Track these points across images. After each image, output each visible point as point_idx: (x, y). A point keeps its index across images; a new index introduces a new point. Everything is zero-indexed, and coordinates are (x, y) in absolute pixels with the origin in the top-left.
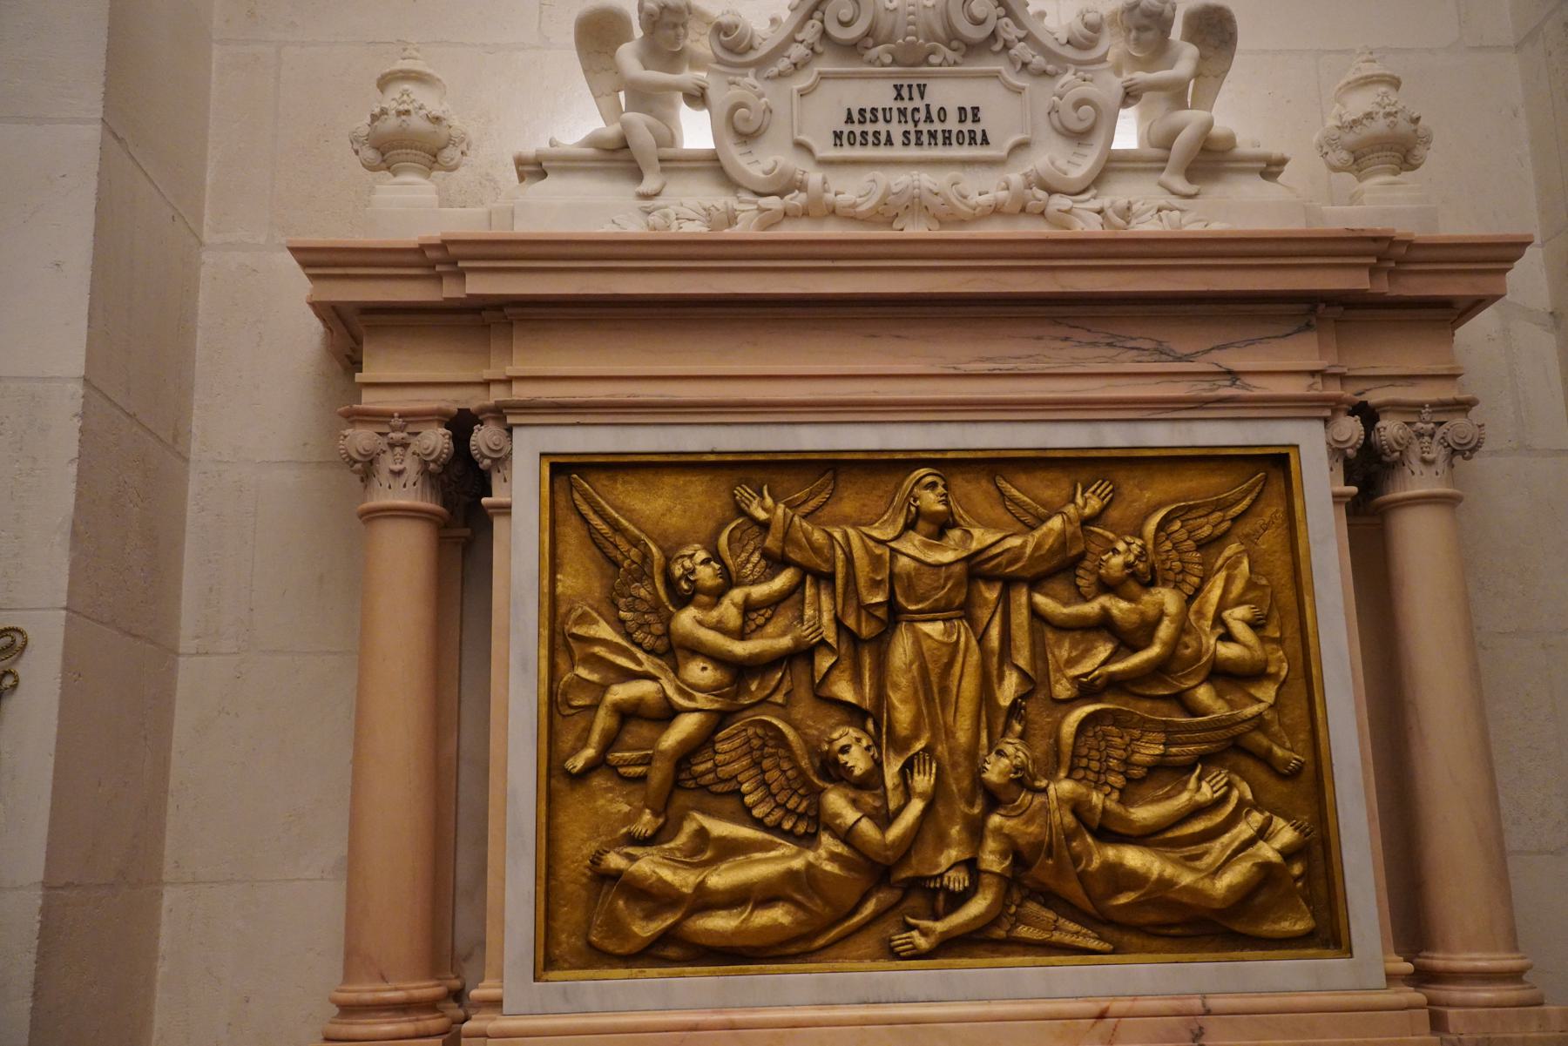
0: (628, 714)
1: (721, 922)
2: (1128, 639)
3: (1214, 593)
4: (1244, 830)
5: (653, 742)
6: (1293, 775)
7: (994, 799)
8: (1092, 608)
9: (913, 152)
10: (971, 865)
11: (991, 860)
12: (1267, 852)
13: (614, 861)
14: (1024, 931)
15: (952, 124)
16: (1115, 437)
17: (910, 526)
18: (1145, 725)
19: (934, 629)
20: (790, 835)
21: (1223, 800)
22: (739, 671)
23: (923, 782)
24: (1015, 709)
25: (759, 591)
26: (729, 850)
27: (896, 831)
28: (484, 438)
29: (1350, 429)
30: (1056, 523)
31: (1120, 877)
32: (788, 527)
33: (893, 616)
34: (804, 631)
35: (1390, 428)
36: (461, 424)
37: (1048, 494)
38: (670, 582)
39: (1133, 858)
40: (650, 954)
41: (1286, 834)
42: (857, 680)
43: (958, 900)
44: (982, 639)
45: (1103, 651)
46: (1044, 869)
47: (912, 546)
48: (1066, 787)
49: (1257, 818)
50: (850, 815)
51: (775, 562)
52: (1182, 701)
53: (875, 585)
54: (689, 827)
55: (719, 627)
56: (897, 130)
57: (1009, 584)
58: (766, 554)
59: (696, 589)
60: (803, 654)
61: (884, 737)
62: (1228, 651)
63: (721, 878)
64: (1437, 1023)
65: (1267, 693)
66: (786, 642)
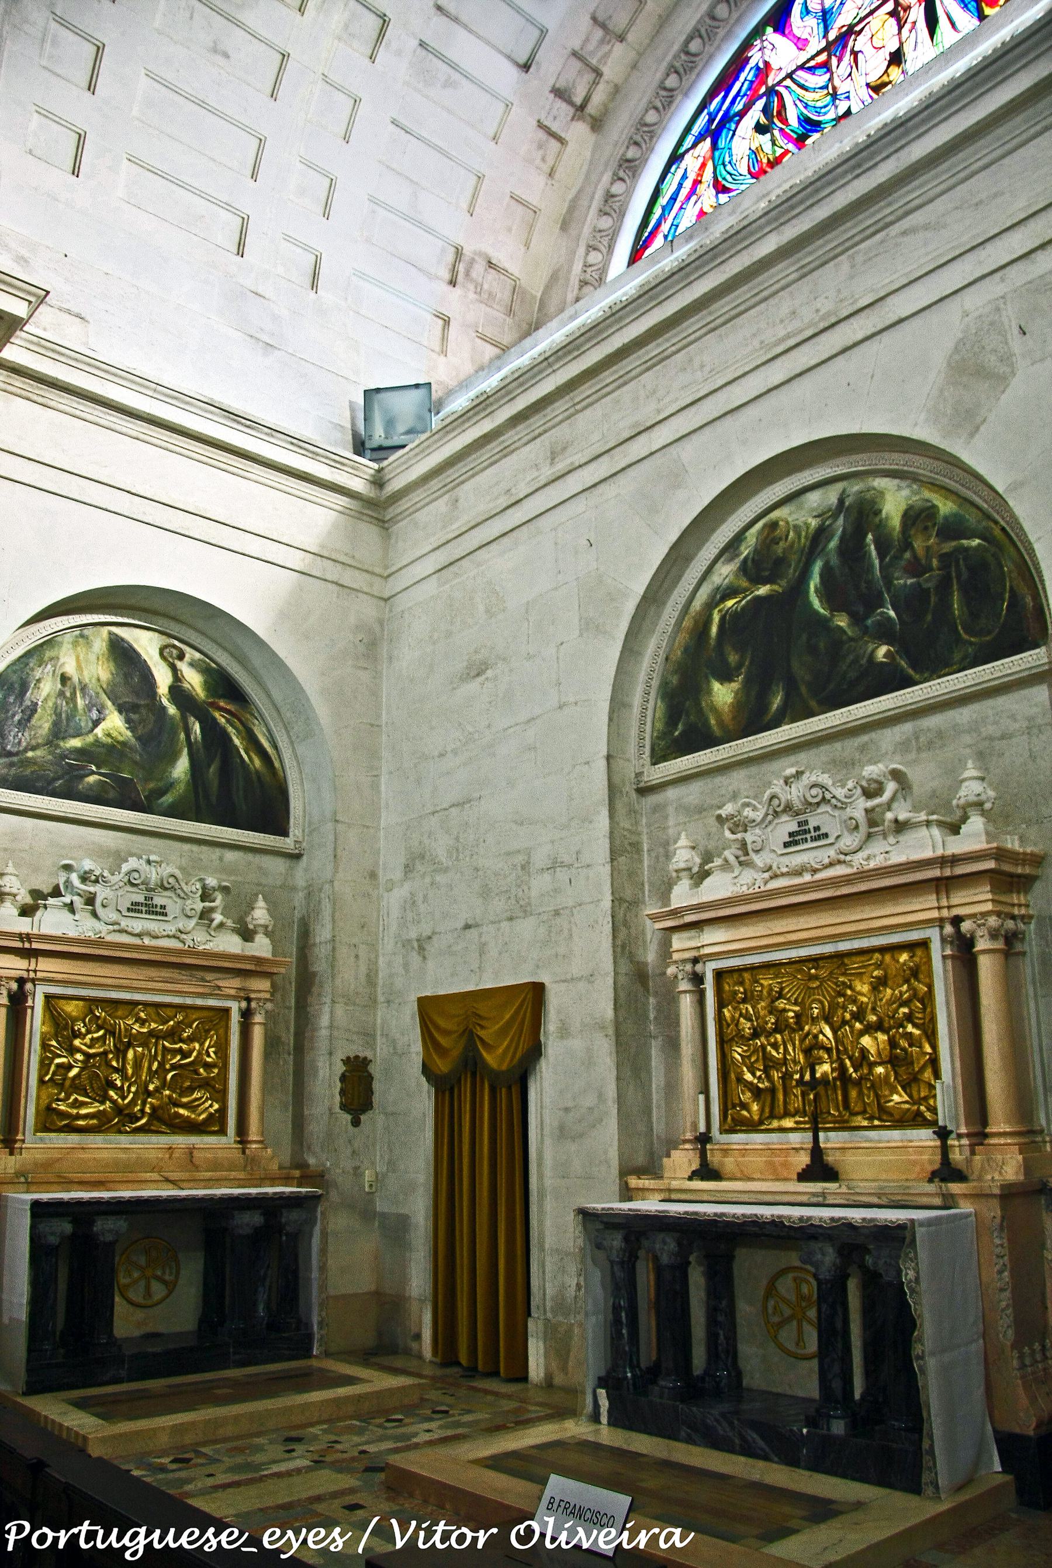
0: (59, 1066)
1: (81, 1123)
2: (185, 1055)
3: (207, 1044)
4: (207, 1104)
5: (66, 1075)
6: (218, 1092)
7: (149, 1094)
8: (177, 1046)
9: (147, 916)
10: (142, 1111)
11: (148, 1110)
12: (212, 1110)
13: (54, 1106)
14: (153, 1128)
15: (158, 910)
16: (189, 1001)
17: (136, 1021)
18: (187, 1078)
19: (140, 1049)
20: (98, 1101)
21: (201, 1098)
22: (88, 1056)
23: (133, 1089)
24: (156, 1071)
25: (95, 1035)
26: (83, 1104)
27: (126, 1101)
28: (29, 986)
29: (244, 1004)
30: (172, 1023)
31: (177, 1114)
32: (105, 1018)
33: (129, 1045)
34: (107, 1047)
35: (253, 1004)
36: (21, 981)
37: (170, 1014)
38: (73, 1030)
39: (181, 1111)
40: (60, 1130)
41: (216, 1106)
42: (118, 1062)
43: (138, 1119)
44: (150, 1052)
45: (178, 1057)
46: (160, 1112)
47: (136, 1026)
48: (167, 1092)
49: (210, 1102)
50: (116, 1097)
51: (99, 1028)
52: (197, 1072)
53: (125, 1037)
54: (73, 1098)
55: (85, 1045)
56: (144, 909)
57: (158, 1038)
58: (97, 1025)
59: (81, 1033)
60: (105, 1053)
61: (125, 1077)
62: (209, 1060)
63: (83, 1111)
64: (244, 1153)
65: (216, 1071)
66: (102, 1050)
